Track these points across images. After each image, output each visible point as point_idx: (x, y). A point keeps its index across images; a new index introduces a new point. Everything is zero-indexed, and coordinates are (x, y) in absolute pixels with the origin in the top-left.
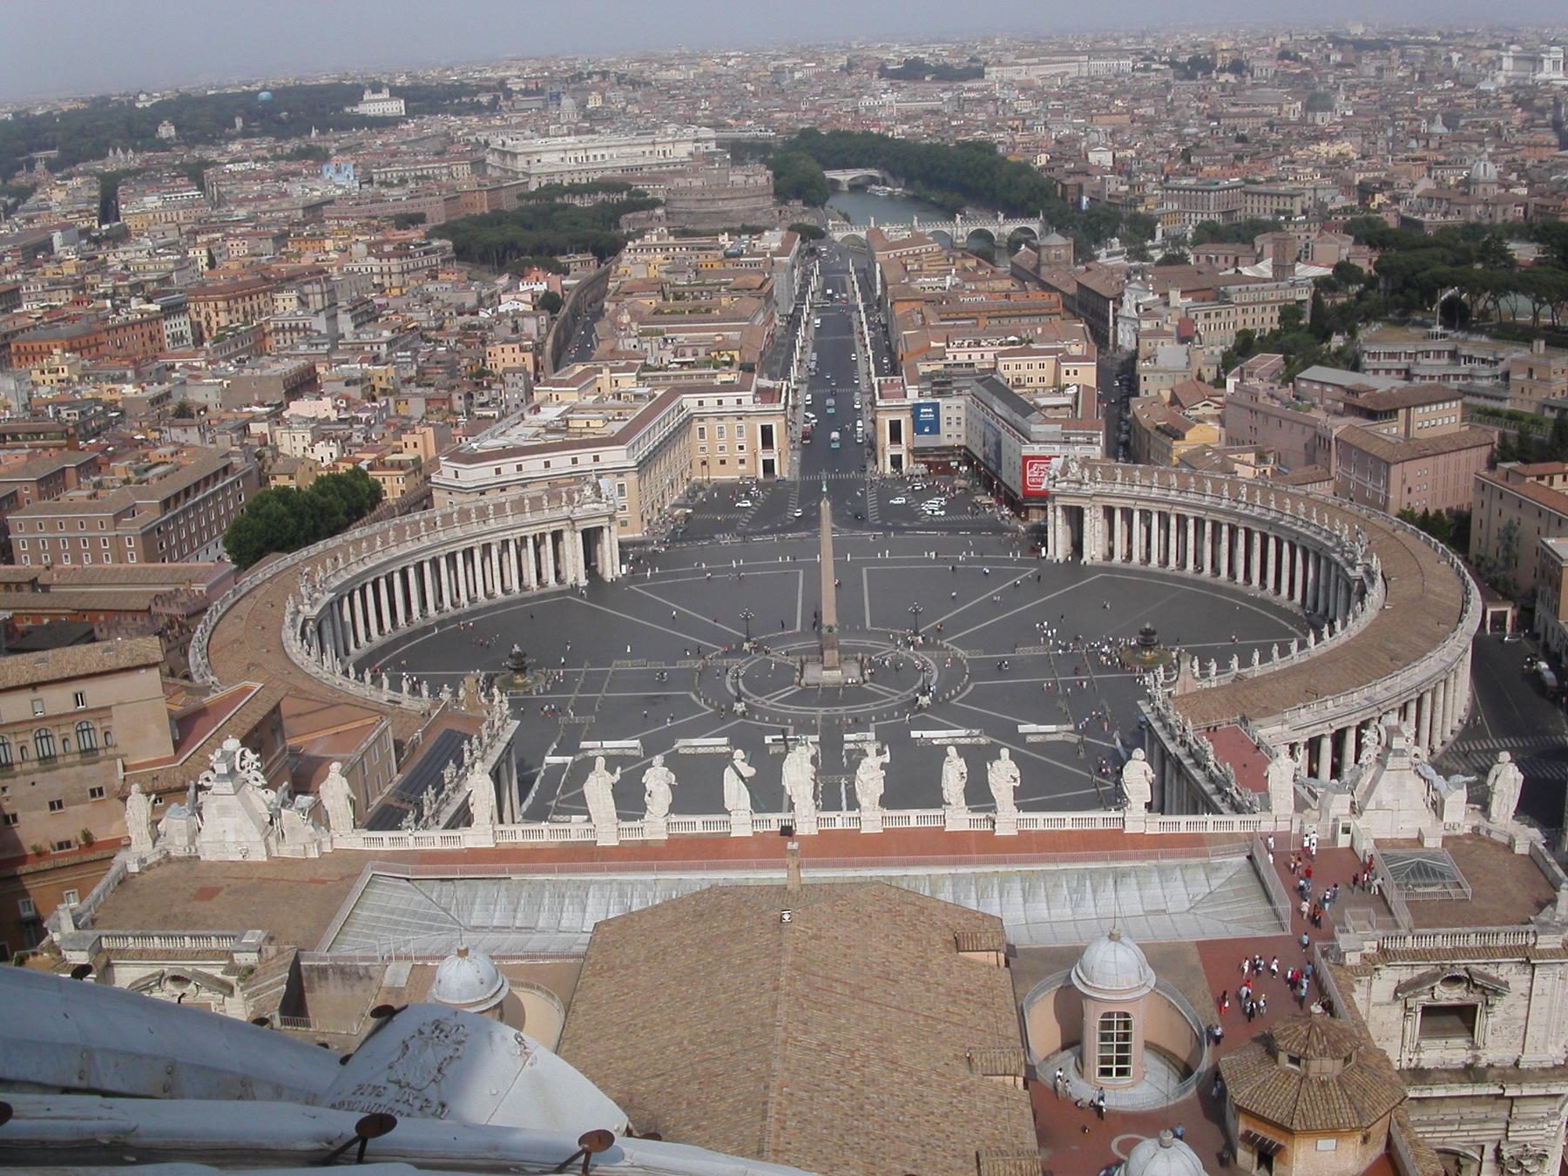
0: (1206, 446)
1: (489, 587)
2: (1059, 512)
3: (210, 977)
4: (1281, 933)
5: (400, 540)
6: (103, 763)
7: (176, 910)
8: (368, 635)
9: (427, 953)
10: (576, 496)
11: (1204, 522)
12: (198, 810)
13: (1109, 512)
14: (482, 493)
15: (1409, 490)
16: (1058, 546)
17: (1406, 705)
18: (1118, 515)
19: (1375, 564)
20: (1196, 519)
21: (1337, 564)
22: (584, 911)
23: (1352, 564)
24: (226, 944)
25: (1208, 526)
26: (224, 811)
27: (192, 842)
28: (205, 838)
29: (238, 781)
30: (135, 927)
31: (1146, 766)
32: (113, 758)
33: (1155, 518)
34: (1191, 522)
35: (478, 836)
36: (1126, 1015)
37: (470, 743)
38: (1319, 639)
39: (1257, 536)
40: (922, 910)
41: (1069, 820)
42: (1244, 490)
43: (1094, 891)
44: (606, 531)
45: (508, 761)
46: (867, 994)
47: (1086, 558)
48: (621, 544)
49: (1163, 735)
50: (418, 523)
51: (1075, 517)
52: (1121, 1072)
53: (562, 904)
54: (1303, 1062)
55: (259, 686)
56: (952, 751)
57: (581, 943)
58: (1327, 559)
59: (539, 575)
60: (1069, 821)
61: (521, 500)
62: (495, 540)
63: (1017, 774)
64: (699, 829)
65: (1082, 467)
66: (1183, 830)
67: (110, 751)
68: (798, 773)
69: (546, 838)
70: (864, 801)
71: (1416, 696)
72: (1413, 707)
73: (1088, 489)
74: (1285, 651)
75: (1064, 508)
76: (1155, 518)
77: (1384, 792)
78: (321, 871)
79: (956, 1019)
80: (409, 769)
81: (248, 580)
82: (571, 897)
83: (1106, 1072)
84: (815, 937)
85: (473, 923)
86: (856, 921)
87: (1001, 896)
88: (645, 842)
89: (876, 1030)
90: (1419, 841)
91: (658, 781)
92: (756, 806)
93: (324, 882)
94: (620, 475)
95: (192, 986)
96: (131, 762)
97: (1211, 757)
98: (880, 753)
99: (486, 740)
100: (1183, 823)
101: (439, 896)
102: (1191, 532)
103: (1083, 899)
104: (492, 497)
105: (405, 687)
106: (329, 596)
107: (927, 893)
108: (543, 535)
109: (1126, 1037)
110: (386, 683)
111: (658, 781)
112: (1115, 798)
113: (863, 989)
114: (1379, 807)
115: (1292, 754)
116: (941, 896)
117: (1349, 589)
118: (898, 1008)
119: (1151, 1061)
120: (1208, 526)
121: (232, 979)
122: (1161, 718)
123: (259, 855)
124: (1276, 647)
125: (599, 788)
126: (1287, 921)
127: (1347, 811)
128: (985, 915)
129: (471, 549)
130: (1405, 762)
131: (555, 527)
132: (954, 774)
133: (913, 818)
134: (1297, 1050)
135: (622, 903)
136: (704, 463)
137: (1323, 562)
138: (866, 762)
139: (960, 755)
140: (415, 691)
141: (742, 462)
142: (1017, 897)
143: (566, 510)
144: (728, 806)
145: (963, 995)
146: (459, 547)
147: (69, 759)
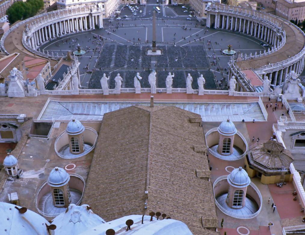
0: (245, 1)
1: (72, 30)
2: (209, 16)
3: (12, 125)
4: (265, 121)
5: (50, 17)
7: (3, 109)
8: (42, 41)
9: (64, 120)
10: (93, 8)
11: (244, 20)
12: (7, 85)
13: (221, 16)
15: (293, 15)
17: (290, 67)
18: (223, 17)
19: (284, 33)
21: (275, 32)
22: (101, 110)
23: (278, 32)
24: (15, 117)
26: (13, 85)
27: (6, 93)
28: (9, 91)
29: (16, 78)
31: (235, 80)
33: (232, 18)
34: (241, 20)
35: (76, 91)
36: (230, 139)
37: (69, 68)
38: (271, 49)
40: (182, 112)
41: (216, 92)
43: (222, 109)
44: (100, 16)
45: (78, 72)
46: (170, 132)
47: (215, 27)
48: (103, 20)
49: (233, 71)
50: (54, 13)
51: (213, 17)
52: (228, 152)
53: (95, 108)
54: (271, 152)
55: (19, 54)
56: (189, 74)
57: (100, 118)
58: (273, 31)
59: (84, 27)
60: (216, 92)
61: (79, 8)
63: (205, 81)
64: (128, 91)
65: (216, 4)
66: (243, 95)
68: (153, 78)
69: (91, 92)
70: (168, 86)
71: (292, 64)
72: (291, 67)
73: (218, 11)
74: (263, 52)
76: (232, 18)
77: (290, 89)
78: (37, 100)
79: (190, 139)
80: (54, 74)
82: (97, 107)
83: (224, 152)
84: (158, 119)
85: (74, 113)
86: (167, 115)
87: (200, 109)
88: (115, 94)
89: (172, 141)
90: (296, 101)
91: (119, 79)
92: (142, 86)
93: (38, 102)
94: (103, 3)
95: (8, 127)
97: (245, 77)
98: (172, 74)
99: (73, 67)
100: (242, 93)
101: (66, 106)
102: (241, 22)
103: (219, 111)
104: (73, 7)
105: (53, 54)
106: (33, 31)
107: (182, 108)
108: (84, 17)
109: (229, 144)
110: (48, 52)
111: (119, 79)
112: (227, 87)
113: (169, 131)
114: (289, 92)
115: (269, 79)
116: (185, 109)
117: (277, 37)
118: (177, 136)
119: (233, 150)
120: (245, 21)
121: (17, 125)
122: (233, 67)
123: (23, 95)
124: (261, 51)
125: (104, 81)
126: (266, 118)
127: (281, 93)
128: (196, 114)
130: (296, 82)
131: (87, 15)
132: (189, 80)
133: (179, 90)
134: (270, 149)
135: (109, 109)
137: (272, 31)
138: (169, 76)
139: (191, 76)
140: (55, 55)
142: (203, 110)
143: (89, 12)
144: (135, 86)
145: (192, 133)
146: (64, 20)
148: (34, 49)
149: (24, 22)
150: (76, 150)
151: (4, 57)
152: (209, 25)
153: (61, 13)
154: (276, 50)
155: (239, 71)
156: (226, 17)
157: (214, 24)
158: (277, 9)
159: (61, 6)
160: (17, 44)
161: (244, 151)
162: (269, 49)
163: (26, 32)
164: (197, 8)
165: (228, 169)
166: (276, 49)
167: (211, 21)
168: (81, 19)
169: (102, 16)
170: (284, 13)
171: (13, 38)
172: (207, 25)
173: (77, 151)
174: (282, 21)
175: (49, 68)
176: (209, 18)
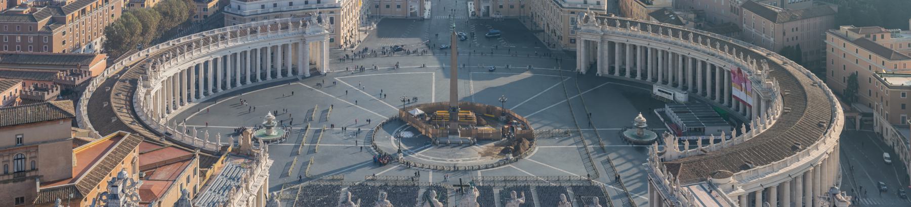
0: (665, 9)
6: (28, 181)
14: (253, 20)
16: (581, 65)
18: (617, 47)
20: (663, 51)
32: (34, 178)
34: (660, 53)
39: (699, 65)
42: (691, 35)
47: (599, 72)
62: (259, 48)
67: (33, 173)
75: (586, 41)
81: (118, 67)
94: (332, 12)
96: (46, 180)
120: (670, 56)
129: (245, 52)
136: (377, 7)
141: (399, 7)
147: (6, 178)
148: (162, 122)
149: (143, 54)
151: (88, 142)
152: (581, 65)
153: (234, 35)
156: (623, 45)
157: (596, 63)
159: (234, 19)
163: (146, 79)
164: (551, 26)
167: (587, 56)
168: (280, 49)
169: (328, 43)
171: (113, 93)
176: (583, 50)
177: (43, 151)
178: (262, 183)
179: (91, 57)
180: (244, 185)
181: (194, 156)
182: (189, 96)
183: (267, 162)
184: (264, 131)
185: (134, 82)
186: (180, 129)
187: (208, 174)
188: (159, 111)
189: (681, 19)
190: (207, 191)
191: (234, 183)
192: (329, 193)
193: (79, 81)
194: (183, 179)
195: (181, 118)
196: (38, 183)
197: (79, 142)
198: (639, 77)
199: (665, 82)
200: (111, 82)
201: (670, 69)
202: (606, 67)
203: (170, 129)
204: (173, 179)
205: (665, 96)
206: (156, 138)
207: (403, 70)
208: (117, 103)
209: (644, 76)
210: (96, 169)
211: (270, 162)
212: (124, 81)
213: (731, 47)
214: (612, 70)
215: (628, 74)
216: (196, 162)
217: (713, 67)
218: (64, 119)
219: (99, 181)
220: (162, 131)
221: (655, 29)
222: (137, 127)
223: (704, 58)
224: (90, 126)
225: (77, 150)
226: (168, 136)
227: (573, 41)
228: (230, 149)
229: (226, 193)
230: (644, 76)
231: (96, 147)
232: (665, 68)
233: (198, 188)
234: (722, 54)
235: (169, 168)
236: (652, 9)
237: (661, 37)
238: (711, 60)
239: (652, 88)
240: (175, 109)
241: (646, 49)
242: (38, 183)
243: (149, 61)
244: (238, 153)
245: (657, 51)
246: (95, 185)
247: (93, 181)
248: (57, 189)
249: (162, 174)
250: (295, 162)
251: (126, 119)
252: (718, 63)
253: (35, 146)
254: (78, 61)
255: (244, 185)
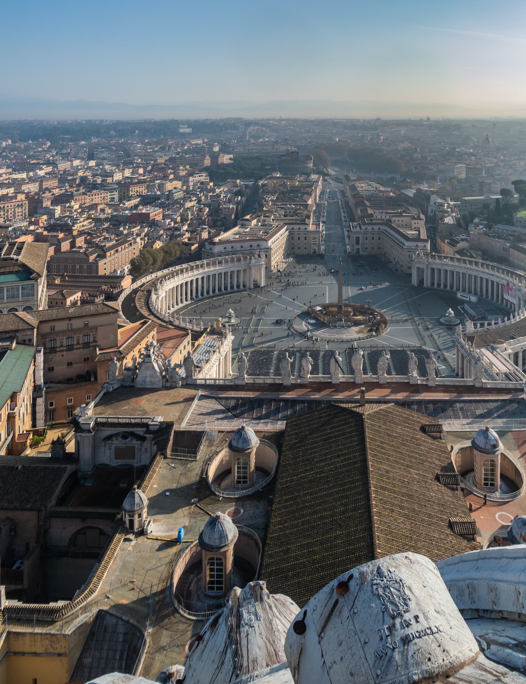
2: (416, 270)
8: (177, 302)
11: (466, 274)
13: (433, 270)
16: (415, 281)
18: (436, 271)
20: (463, 273)
24: (144, 421)
25: (467, 276)
30: (109, 414)
32: (95, 347)
34: (461, 275)
38: (514, 317)
47: (425, 285)
67: (94, 344)
96: (102, 347)
120: (467, 276)
121: (146, 435)
150: (242, 480)
152: (415, 281)
154: (522, 318)
155: (472, 349)
156: (439, 270)
157: (423, 280)
158: (511, 258)
160: (141, 307)
161: (517, 481)
162: (512, 315)
165: (499, 516)
166: (518, 317)
167: (418, 276)
170: (522, 264)
171: (137, 298)
172: (413, 283)
173: (244, 482)
174: (523, 275)
175: (189, 344)
176: (415, 273)
177: (100, 331)
178: (228, 349)
179: (122, 277)
180: (217, 350)
181: (188, 334)
182: (181, 300)
183: (230, 337)
184: (227, 320)
185: (149, 292)
186: (178, 319)
187: (196, 344)
188: (164, 309)
189: (474, 255)
190: (196, 354)
191: (211, 350)
192: (267, 355)
193: (116, 291)
194: (181, 347)
195: (177, 312)
196: (97, 349)
197: (121, 327)
198: (448, 288)
199: (464, 291)
200: (135, 291)
201: (467, 283)
202: (429, 283)
203: (172, 320)
204: (176, 347)
205: (465, 299)
206: (165, 324)
207: (308, 285)
208: (139, 304)
209: (452, 287)
210: (132, 341)
211: (233, 337)
212: (143, 291)
213: (503, 270)
214: (433, 284)
215: (442, 286)
216: (189, 337)
217: (493, 282)
218: (113, 313)
219: (134, 348)
220: (167, 319)
221: (459, 260)
222: (151, 317)
223: (487, 277)
224: (123, 317)
225: (120, 331)
226: (171, 323)
227: (410, 268)
228: (208, 330)
229: (208, 354)
230: (452, 287)
231: (131, 329)
232: (464, 283)
233: (191, 352)
234: (498, 274)
235: (173, 341)
236: (456, 249)
237: (462, 265)
238: (491, 278)
239: (456, 294)
240: (173, 307)
241: (453, 272)
242: (97, 349)
243: (158, 280)
244: (213, 332)
245: (459, 273)
246: (132, 350)
247: (131, 348)
248: (110, 352)
249: (170, 344)
250: (246, 337)
251: (145, 313)
252: (495, 280)
253: (95, 328)
254: (115, 280)
255: (217, 350)
